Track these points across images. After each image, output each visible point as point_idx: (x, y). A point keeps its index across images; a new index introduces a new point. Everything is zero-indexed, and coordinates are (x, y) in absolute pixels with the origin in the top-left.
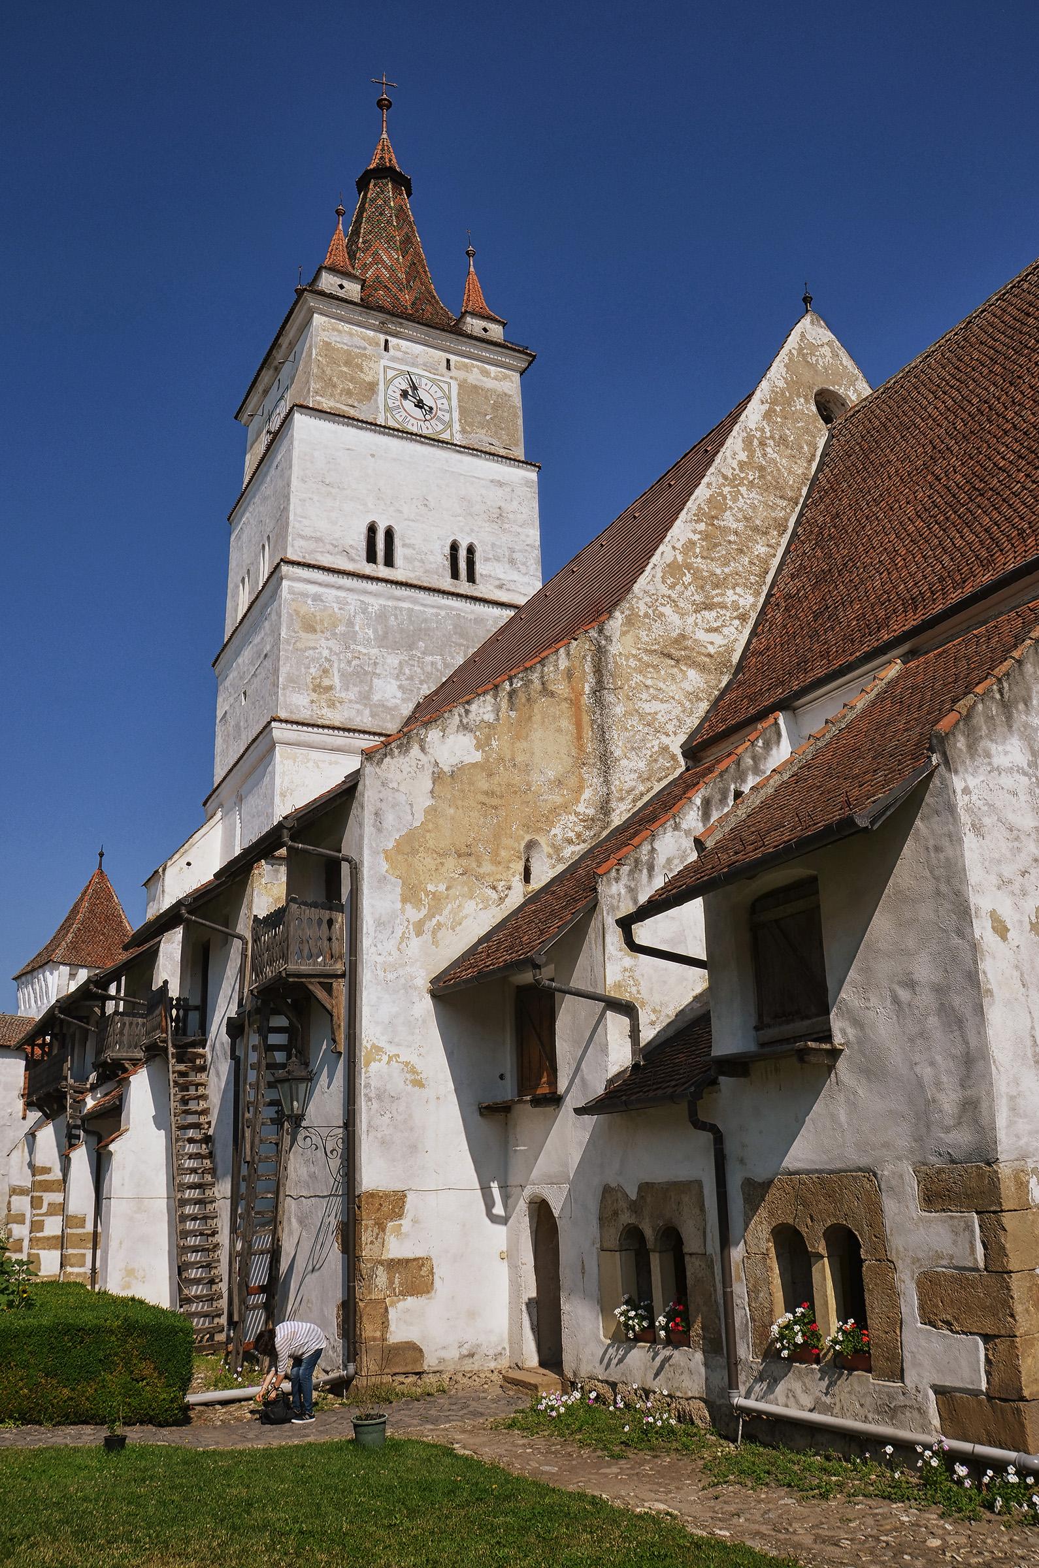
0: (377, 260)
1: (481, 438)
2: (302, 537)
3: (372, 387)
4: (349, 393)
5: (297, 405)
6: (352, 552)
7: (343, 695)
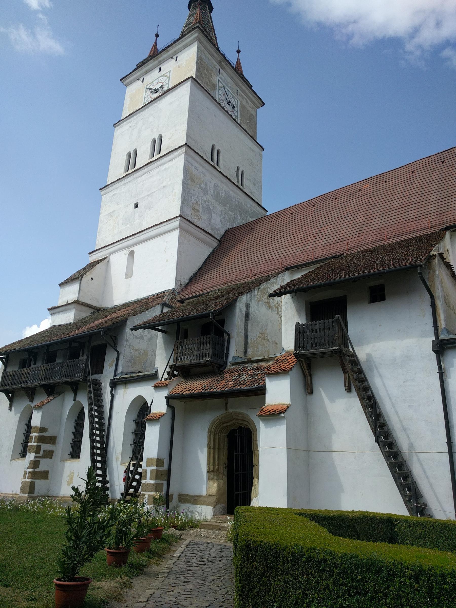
2: (191, 138)
4: (207, 84)
5: (192, 77)
6: (207, 154)
7: (202, 216)
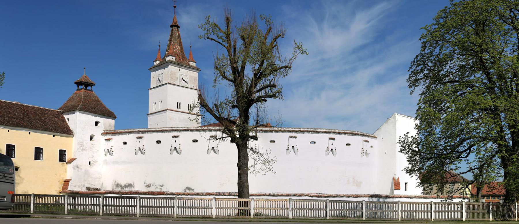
0: (176, 48)
3: (177, 78)
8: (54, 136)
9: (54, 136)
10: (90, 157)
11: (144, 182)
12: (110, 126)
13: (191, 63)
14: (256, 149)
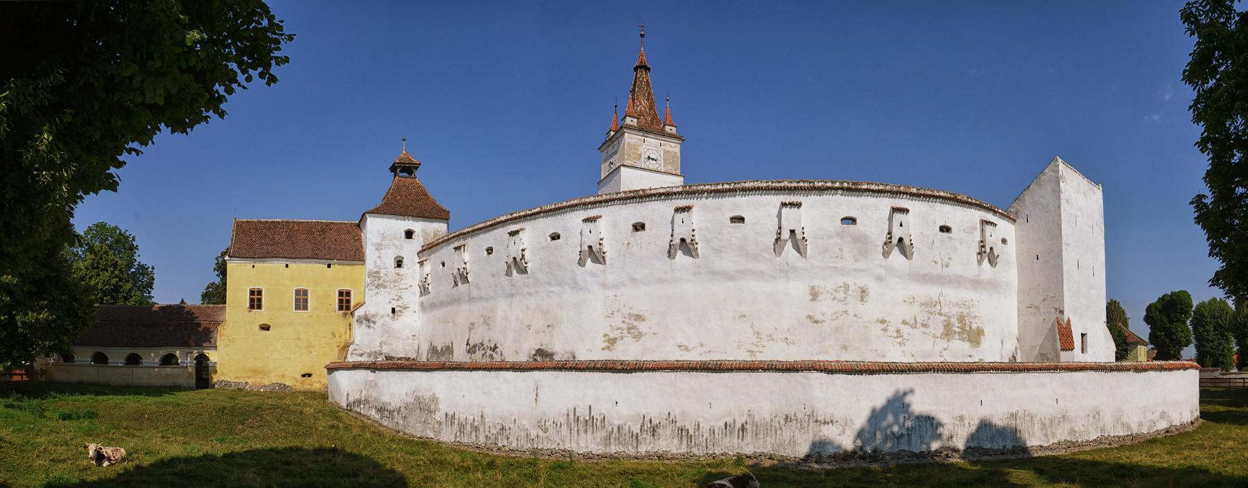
1: (669, 168)
3: (640, 155)
4: (634, 158)
8: (329, 266)
9: (329, 266)
10: (393, 299)
11: (466, 343)
12: (435, 235)
13: (668, 128)
14: (692, 240)
